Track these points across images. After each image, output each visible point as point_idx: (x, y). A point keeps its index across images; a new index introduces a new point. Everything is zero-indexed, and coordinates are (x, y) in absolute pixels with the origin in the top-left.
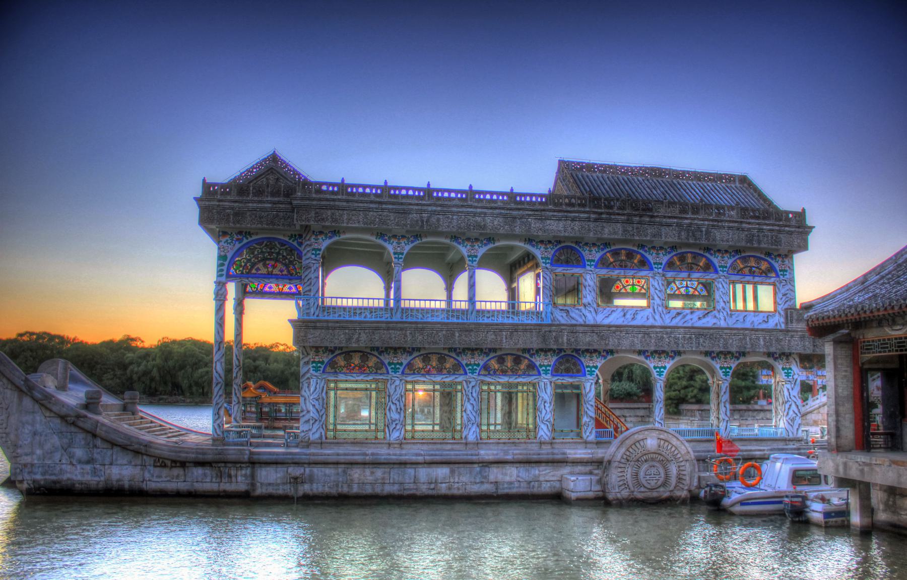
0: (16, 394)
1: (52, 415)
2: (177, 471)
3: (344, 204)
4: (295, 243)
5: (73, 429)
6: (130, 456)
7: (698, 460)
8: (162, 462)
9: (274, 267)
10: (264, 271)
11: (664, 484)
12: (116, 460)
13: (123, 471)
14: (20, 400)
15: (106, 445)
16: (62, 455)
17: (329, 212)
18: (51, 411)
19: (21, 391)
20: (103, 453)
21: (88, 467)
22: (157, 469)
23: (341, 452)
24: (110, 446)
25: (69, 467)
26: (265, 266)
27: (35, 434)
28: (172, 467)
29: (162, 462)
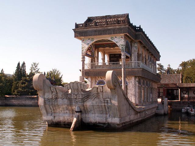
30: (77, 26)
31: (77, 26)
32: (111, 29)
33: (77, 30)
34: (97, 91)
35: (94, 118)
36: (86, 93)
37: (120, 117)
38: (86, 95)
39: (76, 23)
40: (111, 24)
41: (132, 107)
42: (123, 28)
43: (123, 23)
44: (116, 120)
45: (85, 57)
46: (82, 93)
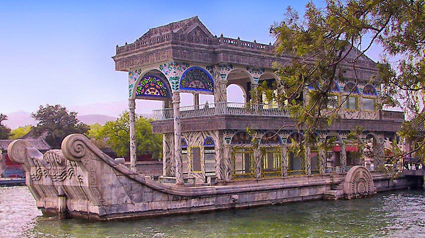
0: (99, 163)
1: (120, 174)
2: (184, 202)
3: (242, 52)
4: (209, 71)
5: (133, 182)
6: (163, 194)
7: (375, 181)
8: (177, 198)
9: (199, 84)
10: (194, 86)
11: (365, 192)
12: (155, 198)
13: (159, 204)
14: (102, 166)
15: (149, 190)
16: (128, 198)
17: (235, 56)
18: (119, 171)
19: (101, 159)
20: (148, 195)
21: (141, 204)
22: (175, 201)
23: (238, 186)
24: (151, 191)
25: (132, 205)
26: (195, 83)
27: (112, 186)
28: (181, 200)
29: (177, 198)
30: (119, 50)
31: (119, 50)
32: (153, 51)
33: (117, 59)
34: (71, 165)
35: (77, 206)
36: (62, 168)
37: (102, 203)
38: (63, 171)
39: (117, 46)
40: (154, 44)
41: (148, 187)
42: (167, 48)
43: (167, 40)
44: (95, 209)
45: (136, 100)
46: (60, 168)
